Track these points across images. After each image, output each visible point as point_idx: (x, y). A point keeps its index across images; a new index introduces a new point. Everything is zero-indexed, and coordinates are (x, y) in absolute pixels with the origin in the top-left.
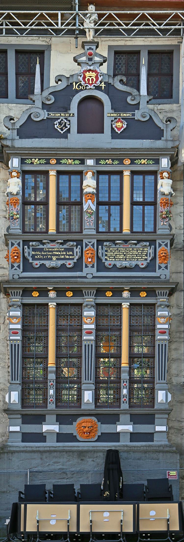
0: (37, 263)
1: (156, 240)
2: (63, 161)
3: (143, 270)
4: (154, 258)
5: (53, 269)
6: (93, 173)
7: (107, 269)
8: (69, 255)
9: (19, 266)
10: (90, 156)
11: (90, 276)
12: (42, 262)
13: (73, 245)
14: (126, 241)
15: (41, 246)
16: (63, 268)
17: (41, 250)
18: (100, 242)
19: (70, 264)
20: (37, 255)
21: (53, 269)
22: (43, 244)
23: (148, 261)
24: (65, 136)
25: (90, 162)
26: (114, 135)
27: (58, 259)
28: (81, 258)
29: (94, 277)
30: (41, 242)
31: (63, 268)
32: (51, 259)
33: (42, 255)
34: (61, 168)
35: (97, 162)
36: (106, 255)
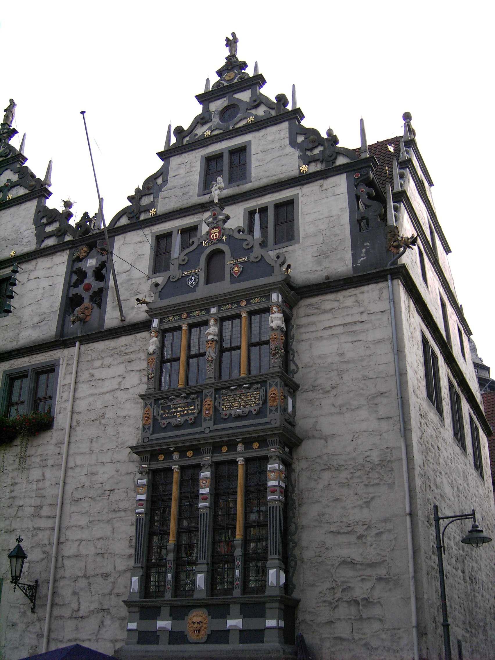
1: (267, 381)
2: (193, 314)
4: (265, 402)
5: (178, 427)
6: (216, 320)
7: (225, 420)
9: (149, 429)
10: (213, 304)
11: (207, 431)
12: (169, 420)
13: (194, 399)
14: (240, 386)
15: (169, 404)
20: (165, 414)
22: (171, 400)
23: (260, 406)
26: (234, 280)
27: (182, 415)
28: (200, 411)
32: (176, 416)
33: (170, 413)
34: (191, 321)
35: (219, 310)
36: (223, 405)
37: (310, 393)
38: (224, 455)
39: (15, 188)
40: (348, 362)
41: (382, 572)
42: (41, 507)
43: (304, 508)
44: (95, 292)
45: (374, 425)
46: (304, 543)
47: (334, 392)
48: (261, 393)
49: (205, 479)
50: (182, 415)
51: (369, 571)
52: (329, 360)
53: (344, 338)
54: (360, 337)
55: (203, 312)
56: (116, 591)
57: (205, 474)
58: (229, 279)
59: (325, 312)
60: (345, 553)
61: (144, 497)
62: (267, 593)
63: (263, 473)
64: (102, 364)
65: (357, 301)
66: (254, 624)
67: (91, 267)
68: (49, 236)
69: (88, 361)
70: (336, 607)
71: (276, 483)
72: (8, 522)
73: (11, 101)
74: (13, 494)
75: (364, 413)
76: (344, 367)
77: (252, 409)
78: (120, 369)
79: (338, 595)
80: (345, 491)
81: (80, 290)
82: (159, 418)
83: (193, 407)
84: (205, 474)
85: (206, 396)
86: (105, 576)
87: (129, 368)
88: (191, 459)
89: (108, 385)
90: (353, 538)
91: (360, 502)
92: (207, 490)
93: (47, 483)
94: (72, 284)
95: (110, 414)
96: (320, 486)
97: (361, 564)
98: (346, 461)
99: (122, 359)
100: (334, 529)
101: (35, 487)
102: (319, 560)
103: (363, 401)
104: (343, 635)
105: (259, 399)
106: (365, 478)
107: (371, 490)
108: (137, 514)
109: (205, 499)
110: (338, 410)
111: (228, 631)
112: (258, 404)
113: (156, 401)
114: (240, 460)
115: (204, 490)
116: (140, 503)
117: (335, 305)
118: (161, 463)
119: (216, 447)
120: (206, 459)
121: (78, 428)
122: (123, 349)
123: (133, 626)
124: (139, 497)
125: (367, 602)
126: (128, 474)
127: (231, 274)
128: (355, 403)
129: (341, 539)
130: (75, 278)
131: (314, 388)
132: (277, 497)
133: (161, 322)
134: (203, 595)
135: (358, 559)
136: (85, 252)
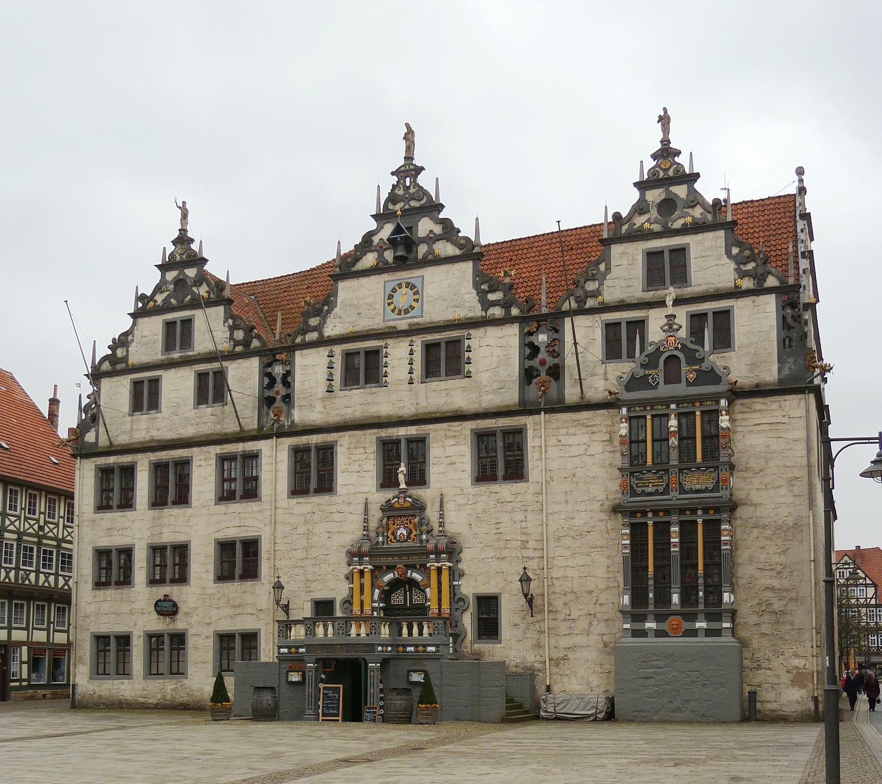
0: (639, 490)
1: (718, 467)
2: (655, 407)
3: (711, 491)
4: (718, 482)
5: (650, 494)
6: (675, 415)
8: (660, 482)
9: (627, 493)
11: (674, 499)
12: (643, 489)
13: (663, 474)
14: (698, 468)
15: (642, 476)
16: (657, 493)
17: (642, 479)
18: (681, 470)
19: (661, 489)
20: (639, 483)
21: (650, 494)
22: (644, 474)
24: (656, 387)
25: (673, 406)
26: (689, 384)
27: (653, 486)
28: (668, 485)
29: (677, 499)
30: (641, 472)
31: (657, 493)
33: (643, 483)
34: (654, 413)
35: (678, 406)
36: (685, 481)
37: (744, 473)
38: (688, 517)
39: (441, 241)
40: (771, 453)
41: (794, 595)
42: (527, 542)
43: (739, 552)
44: (550, 368)
45: (790, 499)
46: (739, 574)
47: (762, 474)
48: (715, 475)
49: (674, 532)
50: (653, 486)
51: (784, 594)
52: (758, 450)
53: (770, 434)
54: (782, 435)
55: (664, 407)
56: (599, 602)
57: (675, 529)
58: (685, 383)
59: (755, 411)
60: (769, 582)
61: (628, 542)
62: (723, 607)
63: (719, 533)
64: (568, 433)
65: (780, 406)
66: (715, 625)
67: (543, 342)
68: (495, 304)
69: (553, 429)
70: (762, 615)
71: (728, 538)
72: (498, 552)
73: (407, 125)
74: (499, 531)
75: (783, 491)
76: (769, 455)
77: (708, 486)
78: (585, 438)
79: (763, 608)
80: (769, 543)
81: (535, 363)
82: (635, 486)
83: (661, 480)
84: (675, 529)
85: (672, 473)
86: (590, 592)
87: (592, 439)
88: (662, 518)
89: (576, 451)
90: (774, 573)
91: (779, 551)
92: (677, 540)
93: (529, 524)
94: (526, 357)
95: (579, 474)
96: (751, 538)
97: (780, 590)
98: (769, 522)
99: (585, 430)
100: (761, 567)
101: (519, 526)
102: (751, 585)
103: (782, 482)
104: (766, 632)
105: (713, 479)
106: (782, 535)
107: (786, 543)
108: (624, 553)
109: (675, 546)
110: (764, 487)
111: (697, 629)
112: (713, 483)
113: (632, 473)
114: (700, 521)
115: (675, 540)
116: (625, 547)
117: (764, 407)
118: (639, 519)
119: (682, 511)
120: (675, 518)
121: (552, 483)
122: (585, 421)
123: (627, 626)
124: (624, 542)
125: (783, 612)
126: (601, 520)
127: (687, 379)
128: (777, 484)
129: (765, 573)
130: (528, 351)
131: (747, 469)
132: (728, 547)
133: (629, 410)
134: (678, 608)
135: (778, 587)
136: (536, 327)
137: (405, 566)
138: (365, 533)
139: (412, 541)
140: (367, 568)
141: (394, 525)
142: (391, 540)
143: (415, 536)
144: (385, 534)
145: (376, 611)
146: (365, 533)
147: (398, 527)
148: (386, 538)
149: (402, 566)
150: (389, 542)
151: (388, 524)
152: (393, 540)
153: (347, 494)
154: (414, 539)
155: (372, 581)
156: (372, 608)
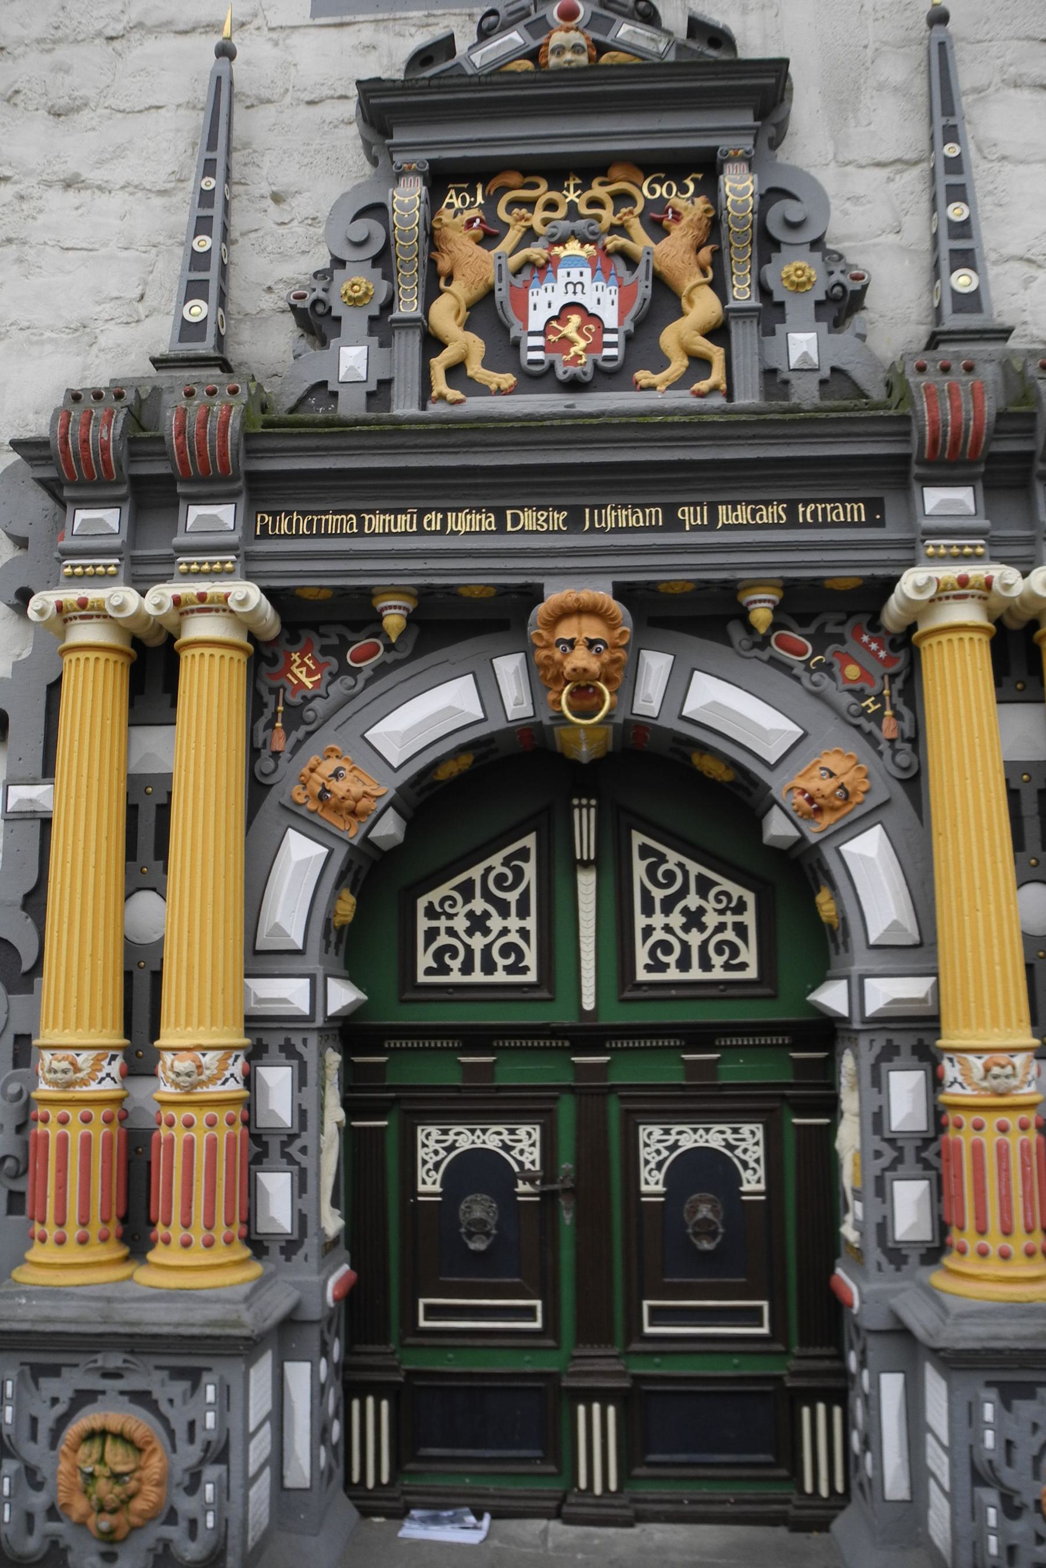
137: (622, 592)
138: (197, 310)
139: (681, 383)
140: (204, 605)
141: (489, 238)
142: (456, 372)
143: (718, 333)
144: (408, 307)
145: (290, 1052)
146: (197, 310)
147: (536, 252)
148: (409, 345)
149: (600, 591)
150: (440, 385)
151: (432, 239)
152: (475, 369)
153: (47, 44)
154: (699, 364)
155: (254, 752)
156: (254, 1023)
